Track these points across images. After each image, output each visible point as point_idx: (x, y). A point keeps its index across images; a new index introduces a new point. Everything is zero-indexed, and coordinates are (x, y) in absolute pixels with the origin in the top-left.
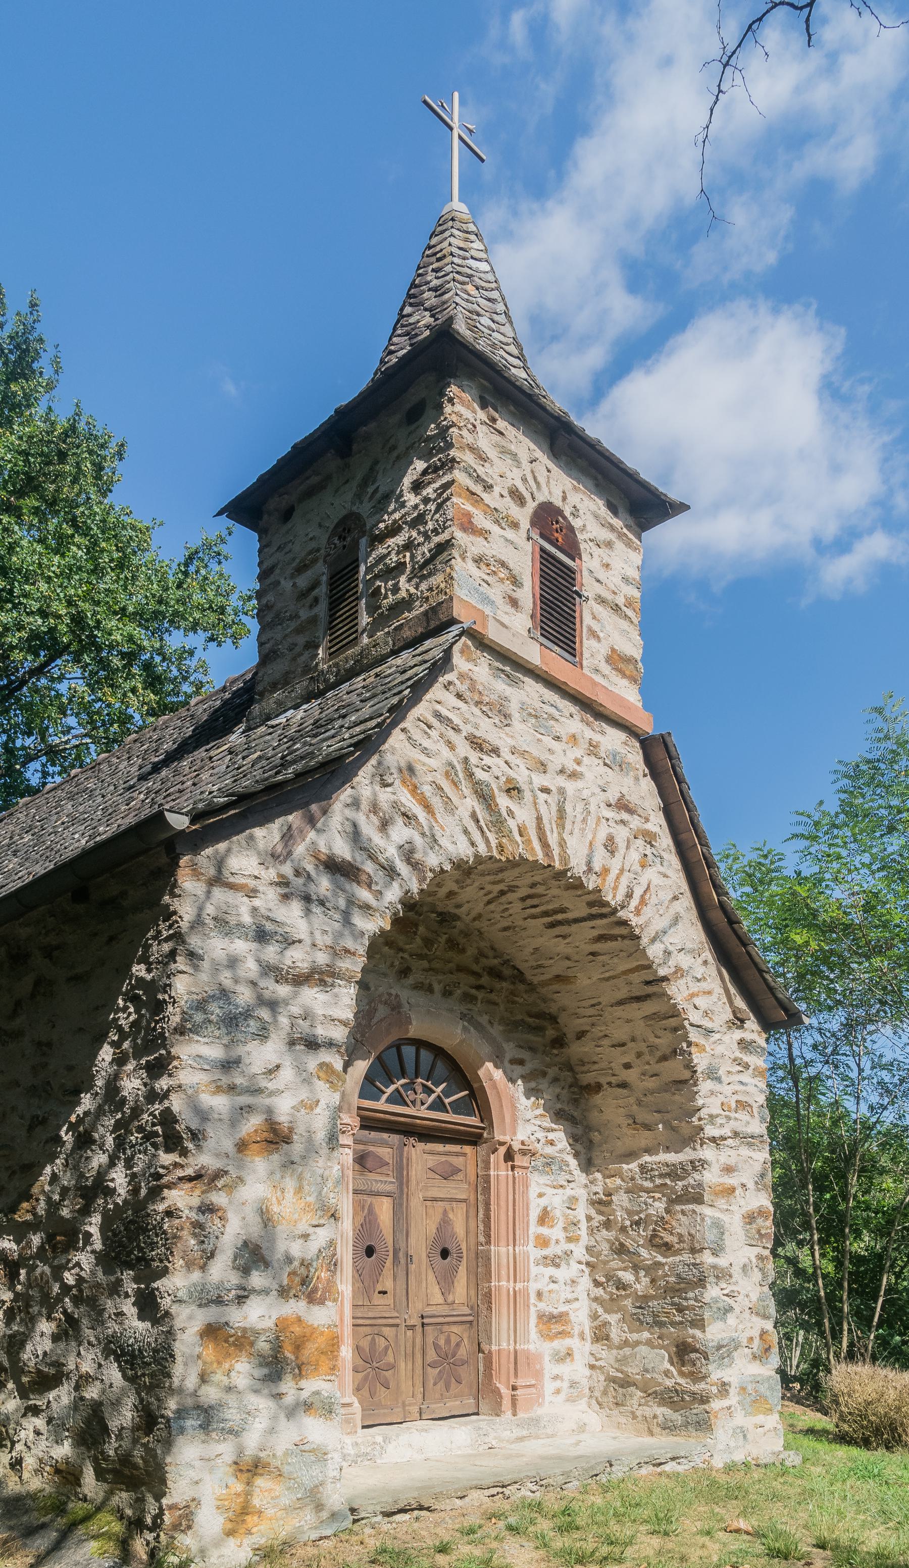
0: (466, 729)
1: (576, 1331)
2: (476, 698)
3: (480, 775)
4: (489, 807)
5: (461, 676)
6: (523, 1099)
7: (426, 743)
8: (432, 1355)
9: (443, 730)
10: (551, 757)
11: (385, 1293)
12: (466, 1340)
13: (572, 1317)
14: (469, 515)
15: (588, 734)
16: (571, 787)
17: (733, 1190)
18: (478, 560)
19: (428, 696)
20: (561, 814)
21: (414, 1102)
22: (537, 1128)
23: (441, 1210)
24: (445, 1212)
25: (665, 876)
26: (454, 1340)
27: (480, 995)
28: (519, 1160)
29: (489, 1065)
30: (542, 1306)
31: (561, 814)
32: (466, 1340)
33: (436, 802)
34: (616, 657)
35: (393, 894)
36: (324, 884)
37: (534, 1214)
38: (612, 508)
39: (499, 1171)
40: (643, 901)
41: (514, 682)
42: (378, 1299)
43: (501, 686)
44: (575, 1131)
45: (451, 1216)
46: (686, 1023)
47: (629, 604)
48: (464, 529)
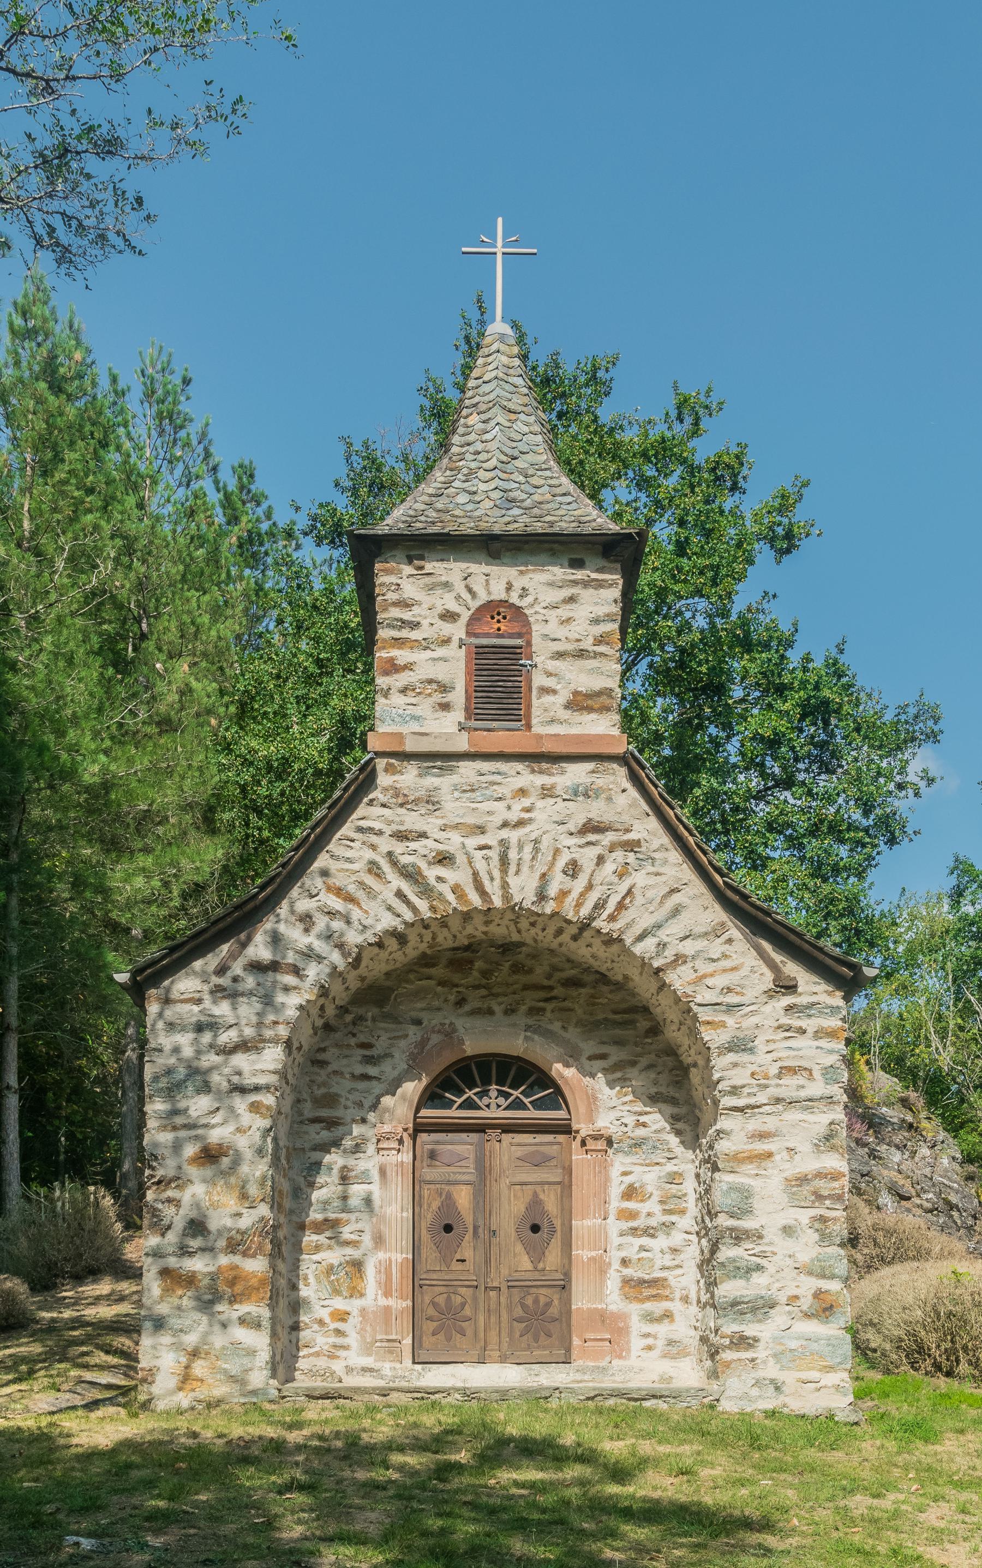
0: (388, 830)
1: (678, 1295)
2: (400, 801)
3: (405, 860)
4: (416, 882)
5: (386, 789)
6: (607, 1090)
7: (349, 854)
8: (519, 1312)
9: (365, 839)
11: (463, 1261)
12: (556, 1302)
13: (672, 1282)
14: (391, 660)
15: (541, 780)
16: (513, 836)
17: (770, 1155)
18: (404, 691)
19: (354, 816)
20: (504, 861)
21: (488, 1106)
22: (625, 1113)
23: (531, 1193)
24: (535, 1194)
25: (657, 874)
26: (542, 1300)
27: (549, 1006)
28: (591, 1145)
29: (558, 1066)
30: (628, 1272)
31: (504, 861)
32: (556, 1302)
33: (360, 895)
34: (579, 698)
35: (313, 971)
36: (250, 982)
37: (615, 1191)
38: (577, 564)
39: (578, 1156)
40: (621, 906)
41: (451, 770)
42: (456, 1266)
43: (431, 781)
44: (676, 1110)
45: (542, 1196)
46: (692, 1004)
47: (599, 641)
48: (386, 673)
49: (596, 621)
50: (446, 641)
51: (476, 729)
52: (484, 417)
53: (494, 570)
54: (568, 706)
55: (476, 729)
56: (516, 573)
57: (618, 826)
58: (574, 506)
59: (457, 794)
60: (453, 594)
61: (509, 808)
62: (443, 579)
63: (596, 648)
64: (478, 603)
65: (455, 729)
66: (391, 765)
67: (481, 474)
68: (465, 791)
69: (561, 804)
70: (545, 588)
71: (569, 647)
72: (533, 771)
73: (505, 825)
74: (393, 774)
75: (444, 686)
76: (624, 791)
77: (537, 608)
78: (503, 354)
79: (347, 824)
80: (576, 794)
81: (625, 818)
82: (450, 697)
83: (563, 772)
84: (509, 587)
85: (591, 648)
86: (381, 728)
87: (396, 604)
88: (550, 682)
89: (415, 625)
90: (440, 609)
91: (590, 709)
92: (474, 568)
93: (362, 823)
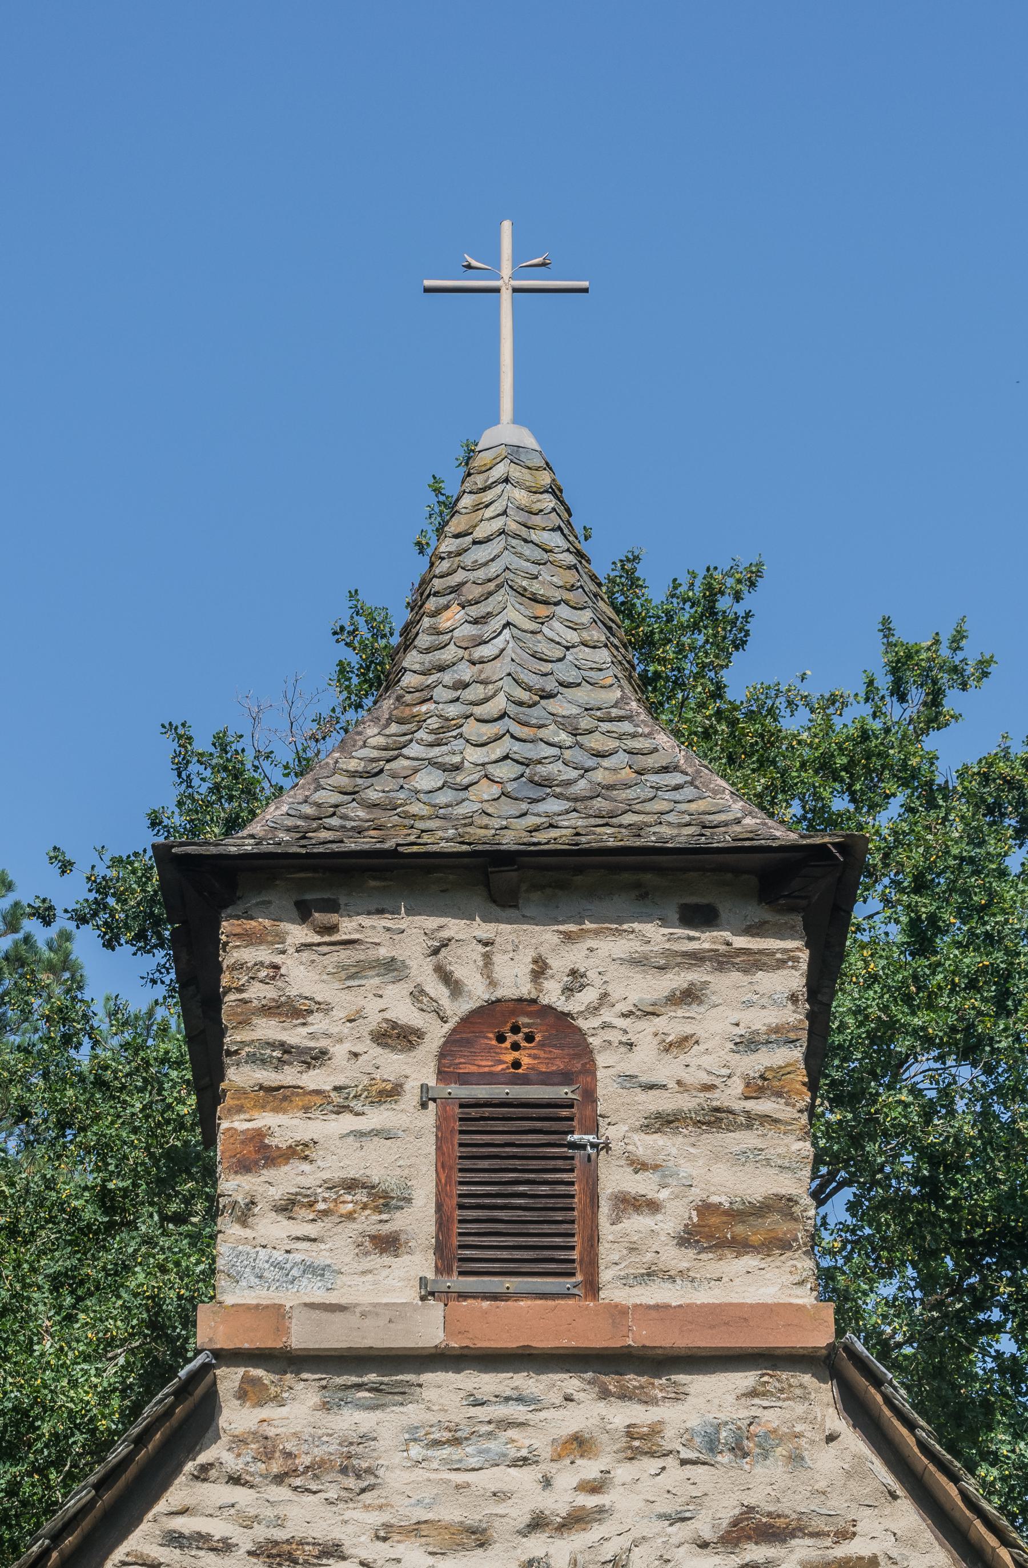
0: (245, 1541)
2: (276, 1468)
5: (240, 1441)
10: (500, 1509)
14: (258, 1137)
18: (287, 1208)
19: (161, 1507)
34: (714, 1220)
41: (403, 1393)
48: (245, 1167)
49: (748, 1043)
50: (390, 1093)
51: (463, 1296)
52: (474, 611)
53: (503, 931)
54: (687, 1238)
55: (463, 1296)
56: (555, 939)
57: (819, 1524)
58: (689, 792)
59: (416, 1451)
60: (407, 987)
61: (547, 1482)
62: (383, 952)
63: (750, 1105)
64: (465, 1006)
65: (411, 1295)
66: (256, 1382)
67: (472, 729)
68: (436, 1443)
69: (676, 1473)
70: (625, 971)
71: (687, 1103)
72: (605, 1394)
73: (537, 1524)
74: (260, 1404)
75: (386, 1195)
76: (831, 1438)
77: (607, 1015)
78: (518, 485)
79: (144, 1527)
80: (712, 1445)
81: (836, 1503)
82: (399, 1221)
83: (679, 1396)
84: (540, 970)
85: (738, 1105)
86: (231, 1295)
87: (270, 1010)
88: (641, 1185)
89: (315, 1058)
90: (374, 1021)
91: (741, 1246)
92: (455, 927)
93: (184, 1524)
